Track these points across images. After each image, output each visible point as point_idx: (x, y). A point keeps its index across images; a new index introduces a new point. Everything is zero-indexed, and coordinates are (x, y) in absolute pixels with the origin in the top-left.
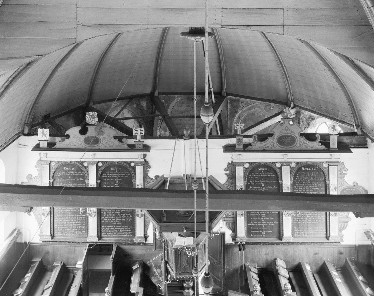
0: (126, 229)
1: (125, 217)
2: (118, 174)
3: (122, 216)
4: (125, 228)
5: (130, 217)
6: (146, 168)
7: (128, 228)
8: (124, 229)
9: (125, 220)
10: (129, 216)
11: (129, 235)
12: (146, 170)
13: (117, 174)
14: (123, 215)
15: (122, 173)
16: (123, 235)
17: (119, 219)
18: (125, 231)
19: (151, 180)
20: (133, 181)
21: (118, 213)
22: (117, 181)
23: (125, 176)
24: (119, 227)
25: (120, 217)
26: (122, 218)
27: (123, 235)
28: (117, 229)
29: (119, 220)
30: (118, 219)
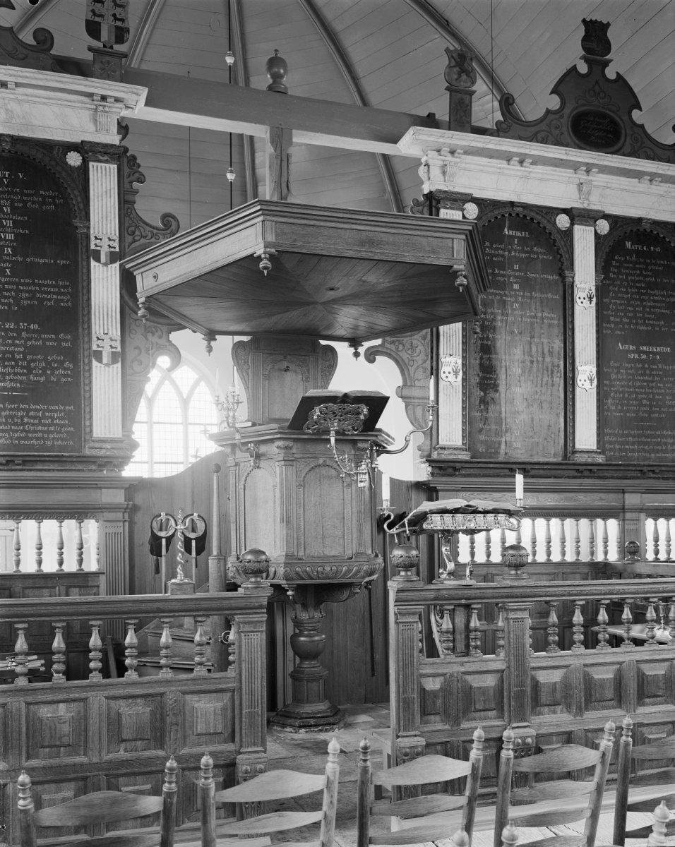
0: (47, 414)
1: (44, 369)
2: (16, 194)
3: (33, 364)
4: (45, 411)
5: (66, 369)
6: (126, 181)
7: (56, 411)
8: (40, 414)
9: (43, 379)
10: (62, 363)
11: (63, 439)
12: (127, 185)
13: (9, 193)
14: (34, 361)
15: (30, 192)
16: (37, 439)
17: (21, 374)
18: (45, 425)
19: (148, 228)
20: (77, 222)
21: (12, 353)
22: (10, 223)
23: (44, 203)
24: (18, 409)
25: (22, 367)
26: (30, 370)
27: (37, 439)
28: (12, 417)
29: (21, 382)
30: (15, 374)
